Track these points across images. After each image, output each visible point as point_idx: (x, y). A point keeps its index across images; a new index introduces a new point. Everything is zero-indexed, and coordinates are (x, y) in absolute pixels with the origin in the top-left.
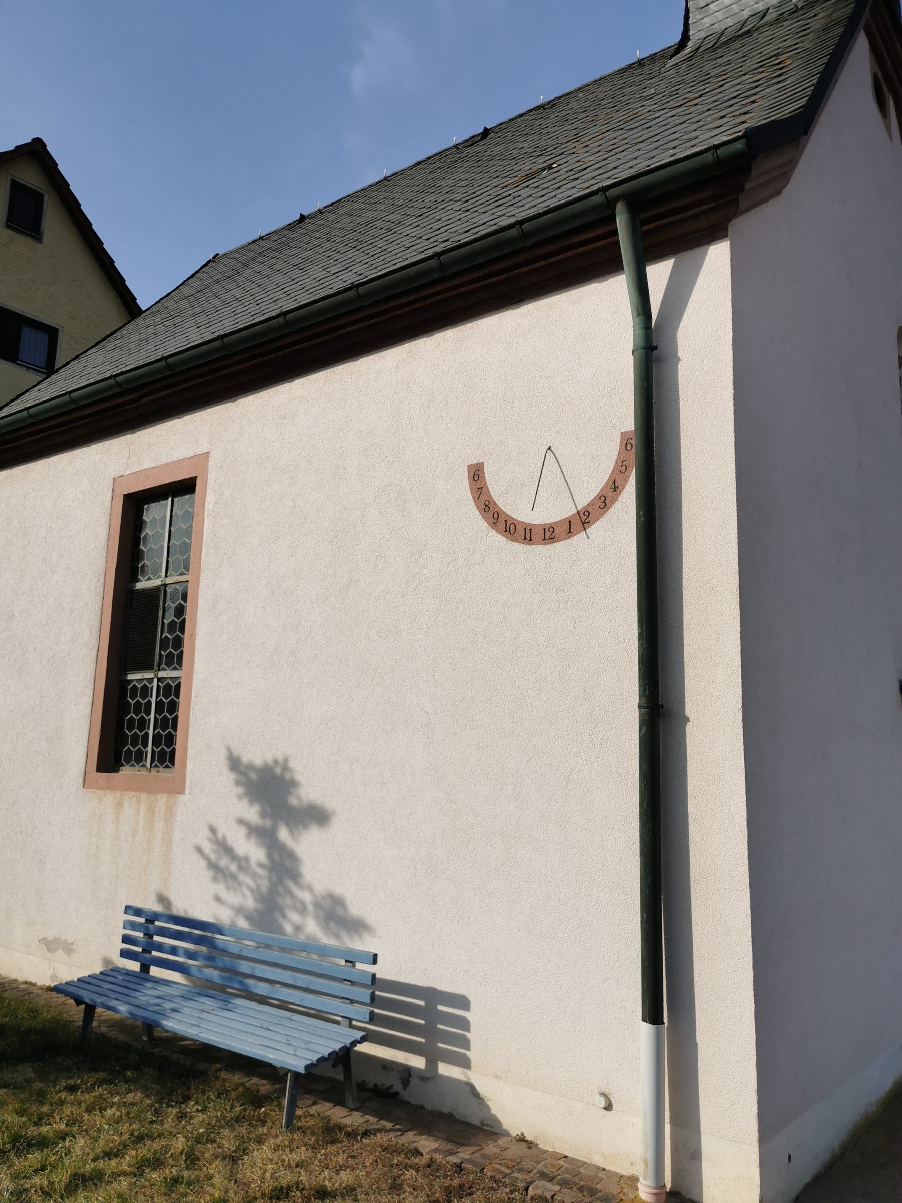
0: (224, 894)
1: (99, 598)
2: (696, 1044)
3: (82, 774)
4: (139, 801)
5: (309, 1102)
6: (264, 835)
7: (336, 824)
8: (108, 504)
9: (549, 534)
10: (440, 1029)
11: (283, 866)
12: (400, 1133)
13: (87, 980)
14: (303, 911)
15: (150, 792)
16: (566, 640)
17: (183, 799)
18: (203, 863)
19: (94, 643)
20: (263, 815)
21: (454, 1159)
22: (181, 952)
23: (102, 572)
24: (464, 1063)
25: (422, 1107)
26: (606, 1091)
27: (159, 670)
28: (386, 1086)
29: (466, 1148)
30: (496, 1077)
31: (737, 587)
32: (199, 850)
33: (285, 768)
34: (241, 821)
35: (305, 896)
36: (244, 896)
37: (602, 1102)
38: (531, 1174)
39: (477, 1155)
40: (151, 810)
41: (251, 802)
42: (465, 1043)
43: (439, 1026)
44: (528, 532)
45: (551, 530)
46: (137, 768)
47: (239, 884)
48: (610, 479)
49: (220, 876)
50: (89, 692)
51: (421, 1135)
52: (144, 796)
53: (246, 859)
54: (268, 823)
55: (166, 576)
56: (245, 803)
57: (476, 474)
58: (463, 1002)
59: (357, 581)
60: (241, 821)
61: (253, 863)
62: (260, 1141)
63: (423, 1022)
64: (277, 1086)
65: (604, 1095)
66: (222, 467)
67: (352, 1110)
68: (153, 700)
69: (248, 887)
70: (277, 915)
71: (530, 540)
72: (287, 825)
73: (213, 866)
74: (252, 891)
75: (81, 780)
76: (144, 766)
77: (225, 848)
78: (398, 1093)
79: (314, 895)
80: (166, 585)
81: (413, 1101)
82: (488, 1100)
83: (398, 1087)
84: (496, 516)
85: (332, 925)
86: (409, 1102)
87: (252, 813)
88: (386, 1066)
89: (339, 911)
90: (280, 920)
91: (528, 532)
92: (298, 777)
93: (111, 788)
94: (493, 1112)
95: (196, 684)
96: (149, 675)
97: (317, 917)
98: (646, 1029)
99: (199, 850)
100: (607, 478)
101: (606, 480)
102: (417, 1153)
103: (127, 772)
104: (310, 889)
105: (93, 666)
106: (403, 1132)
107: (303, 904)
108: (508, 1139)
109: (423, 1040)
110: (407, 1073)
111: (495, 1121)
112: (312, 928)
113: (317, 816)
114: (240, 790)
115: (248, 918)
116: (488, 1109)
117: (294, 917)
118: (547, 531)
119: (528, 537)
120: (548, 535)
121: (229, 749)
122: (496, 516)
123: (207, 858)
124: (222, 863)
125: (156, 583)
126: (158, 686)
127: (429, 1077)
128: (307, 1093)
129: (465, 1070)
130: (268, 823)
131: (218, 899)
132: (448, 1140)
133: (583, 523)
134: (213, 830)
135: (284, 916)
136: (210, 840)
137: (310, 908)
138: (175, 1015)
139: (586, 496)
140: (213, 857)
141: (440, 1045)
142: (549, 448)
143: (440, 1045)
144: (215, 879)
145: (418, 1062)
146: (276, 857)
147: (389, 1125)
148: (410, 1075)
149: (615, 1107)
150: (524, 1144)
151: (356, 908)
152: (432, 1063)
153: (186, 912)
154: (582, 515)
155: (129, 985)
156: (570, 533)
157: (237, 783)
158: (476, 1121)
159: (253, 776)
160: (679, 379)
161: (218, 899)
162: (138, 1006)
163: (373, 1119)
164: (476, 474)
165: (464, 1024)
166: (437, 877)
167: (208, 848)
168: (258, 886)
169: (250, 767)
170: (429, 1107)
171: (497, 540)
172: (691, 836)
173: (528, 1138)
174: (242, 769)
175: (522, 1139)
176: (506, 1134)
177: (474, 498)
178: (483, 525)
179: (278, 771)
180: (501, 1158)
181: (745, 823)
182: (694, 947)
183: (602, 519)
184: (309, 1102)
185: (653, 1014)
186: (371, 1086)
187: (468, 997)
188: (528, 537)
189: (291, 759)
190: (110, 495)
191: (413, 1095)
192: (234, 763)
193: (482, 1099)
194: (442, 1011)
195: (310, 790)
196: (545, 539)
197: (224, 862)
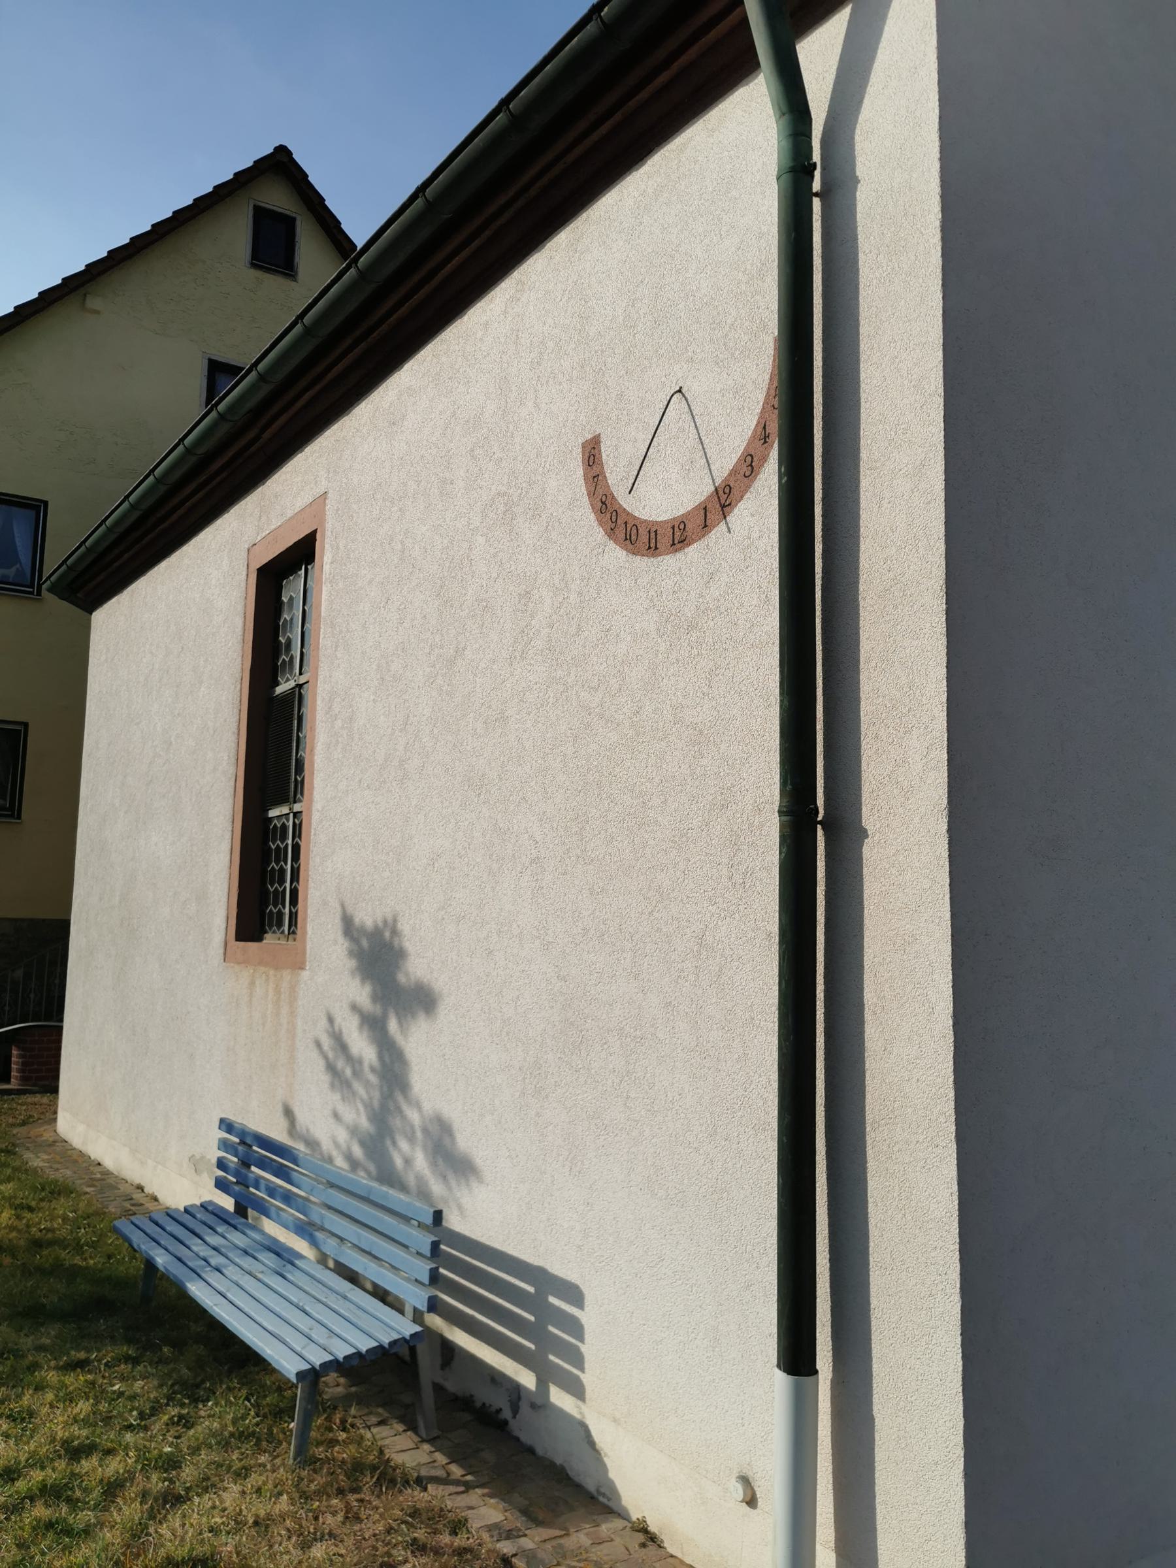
0: (342, 1109)
1: (236, 711)
2: (872, 1419)
3: (223, 944)
4: (267, 980)
5: (374, 1419)
6: (374, 1025)
7: (444, 1011)
8: (243, 584)
9: (678, 535)
10: (550, 1332)
11: (393, 1072)
12: (462, 1489)
13: (175, 1216)
14: (411, 1139)
15: (276, 968)
16: (699, 709)
17: (305, 974)
18: (321, 1063)
19: (232, 770)
20: (375, 998)
21: (506, 1547)
22: (263, 1187)
23: (238, 676)
24: (577, 1390)
25: (531, 1451)
26: (750, 1474)
27: (295, 802)
28: (493, 1409)
29: (540, 1530)
30: (615, 1420)
31: (942, 582)
32: (318, 1044)
33: (395, 932)
34: (354, 1008)
35: (414, 1116)
36: (358, 1113)
37: (738, 1491)
39: (548, 1546)
40: (277, 991)
41: (363, 981)
42: (578, 1360)
43: (551, 1329)
44: (653, 535)
45: (682, 526)
46: (278, 935)
47: (354, 1094)
48: (758, 423)
49: (337, 1083)
50: (228, 835)
51: (491, 1496)
52: (272, 972)
53: (360, 1061)
54: (378, 1010)
55: (301, 674)
56: (357, 981)
57: (592, 454)
58: (574, 1294)
59: (464, 649)
60: (354, 1008)
62: (242, 1474)
63: (532, 1318)
64: (353, 1389)
65: (745, 1481)
66: (337, 510)
67: (423, 1441)
68: (290, 842)
69: (362, 1100)
70: (388, 1143)
71: (656, 548)
72: (397, 1014)
73: (331, 1068)
74: (366, 1106)
75: (222, 951)
76: (283, 932)
77: (342, 1046)
78: (506, 1422)
79: (422, 1116)
80: (300, 686)
82: (606, 1455)
83: (507, 1414)
84: (614, 518)
85: (440, 1162)
86: (518, 1439)
87: (361, 993)
88: (496, 1378)
89: (447, 1141)
90: (391, 1149)
91: (653, 535)
92: (409, 945)
93: (245, 962)
94: (612, 1475)
95: (316, 817)
96: (285, 810)
98: (781, 1380)
99: (318, 1044)
100: (755, 422)
101: (752, 428)
102: (457, 1526)
103: (269, 939)
104: (418, 1106)
105: (231, 801)
106: (469, 1487)
107: (412, 1127)
108: (618, 1523)
109: (533, 1347)
110: (516, 1391)
111: (614, 1493)
112: (421, 1162)
113: (422, 1000)
114: (353, 963)
115: (362, 1144)
116: (604, 1468)
117: (404, 1145)
118: (676, 529)
119: (653, 545)
120: (677, 534)
121: (343, 906)
122: (614, 518)
123: (326, 1058)
124: (339, 1068)
125: (292, 684)
126: (294, 823)
127: (540, 1404)
128: (378, 1406)
129: (579, 1403)
130: (378, 1010)
131: (336, 1116)
132: (525, 1512)
133: (723, 507)
134: (331, 1020)
135: (394, 1143)
136: (328, 1032)
137: (419, 1134)
138: (213, 1278)
139: (725, 462)
140: (331, 1055)
141: (551, 1357)
142: (680, 391)
143: (551, 1357)
144: (332, 1086)
145: (527, 1379)
146: (387, 1060)
147: (456, 1471)
148: (519, 1398)
149: (760, 1502)
150: (641, 1537)
151: (465, 1141)
152: (542, 1383)
153: (308, 1130)
154: (721, 492)
155: (200, 1229)
156: (706, 527)
157: (351, 953)
158: (591, 1486)
159: (365, 943)
160: (859, 216)
161: (336, 1116)
162: (180, 1260)
163: (441, 1458)
164: (592, 454)
165: (577, 1329)
166: (547, 1096)
168: (371, 1098)
169: (362, 930)
170: (540, 1452)
171: (616, 554)
172: (868, 1044)
173: (653, 1528)
174: (355, 934)
175: (642, 1528)
176: (622, 1515)
177: (589, 494)
178: (599, 534)
179: (387, 934)
180: (584, 1556)
181: (951, 1022)
182: (871, 1244)
183: (748, 495)
184: (374, 1419)
185: (796, 1357)
186: (478, 1404)
187: (582, 1287)
188: (653, 545)
189: (400, 918)
190: (245, 573)
191: (524, 1427)
192: (349, 926)
195: (419, 966)
196: (674, 544)
197: (340, 1064)
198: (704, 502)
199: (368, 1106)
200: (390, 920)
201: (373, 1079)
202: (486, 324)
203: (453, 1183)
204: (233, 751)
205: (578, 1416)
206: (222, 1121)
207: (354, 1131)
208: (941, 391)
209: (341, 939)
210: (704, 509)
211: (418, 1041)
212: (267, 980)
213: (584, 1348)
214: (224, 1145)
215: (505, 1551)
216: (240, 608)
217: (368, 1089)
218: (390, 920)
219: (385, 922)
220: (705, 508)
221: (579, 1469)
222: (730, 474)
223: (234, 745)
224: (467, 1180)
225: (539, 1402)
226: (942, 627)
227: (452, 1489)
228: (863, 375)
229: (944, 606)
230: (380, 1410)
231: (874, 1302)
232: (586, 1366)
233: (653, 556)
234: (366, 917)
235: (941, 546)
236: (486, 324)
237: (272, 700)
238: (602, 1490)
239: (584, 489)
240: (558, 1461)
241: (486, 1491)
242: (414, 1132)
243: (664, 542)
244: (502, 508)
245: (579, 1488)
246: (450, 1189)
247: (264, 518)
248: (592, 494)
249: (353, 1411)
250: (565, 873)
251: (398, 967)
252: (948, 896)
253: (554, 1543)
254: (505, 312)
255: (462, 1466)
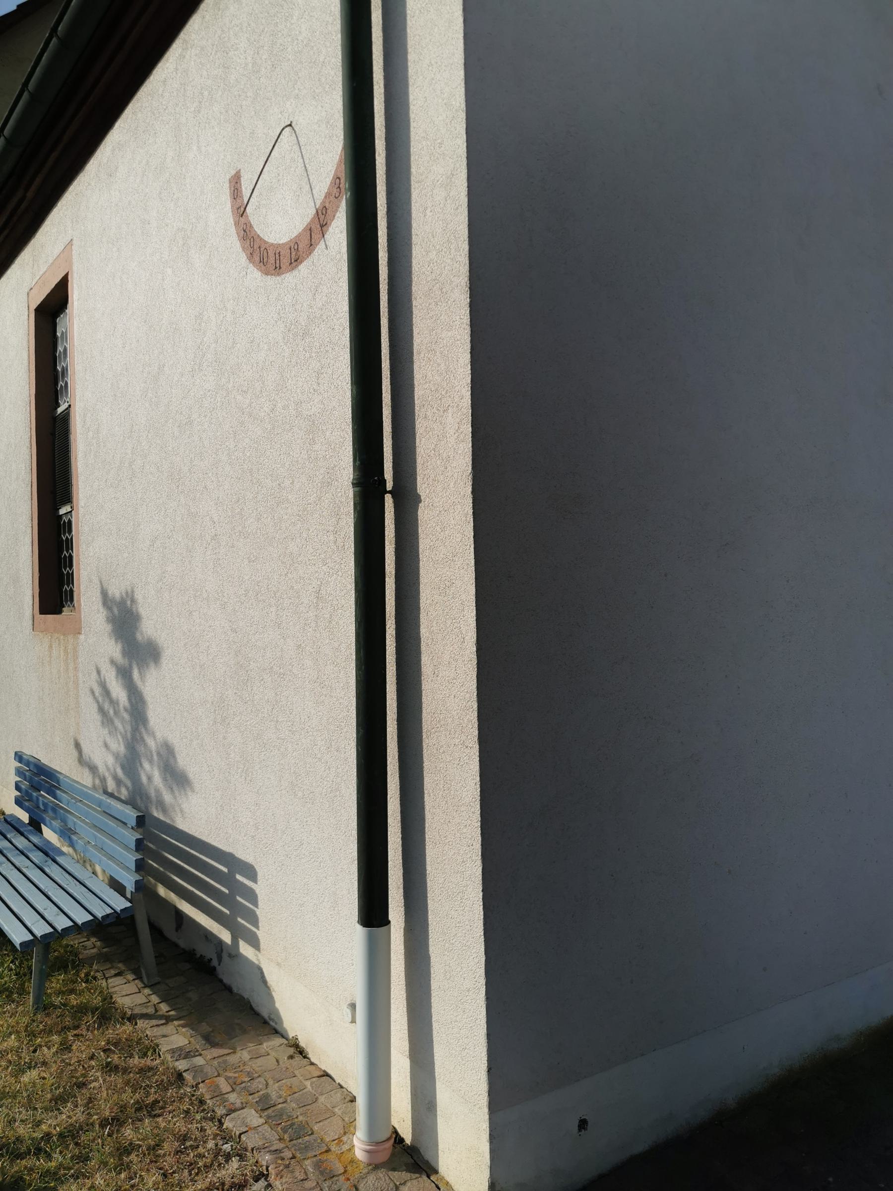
1: (28, 429)
6: (124, 674)
7: (165, 660)
8: (26, 323)
12: (163, 1021)
14: (151, 762)
18: (95, 706)
20: (125, 653)
21: (181, 1065)
23: (27, 400)
24: (255, 943)
25: (229, 989)
28: (206, 959)
29: (213, 1050)
30: (278, 964)
32: (93, 692)
33: (133, 601)
35: (151, 743)
36: (119, 744)
38: (251, 1097)
42: (255, 921)
47: (116, 729)
51: (183, 1026)
56: (113, 642)
58: (250, 872)
59: (164, 365)
60: (113, 662)
61: (121, 706)
69: (121, 733)
73: (101, 710)
74: (123, 738)
75: (31, 622)
77: (107, 692)
79: (156, 743)
81: (225, 981)
83: (215, 963)
85: (168, 776)
86: (221, 981)
87: (113, 649)
88: (208, 936)
89: (172, 761)
90: (139, 769)
94: (277, 1005)
97: (159, 767)
98: (359, 932)
99: (93, 692)
104: (153, 735)
106: (168, 1019)
109: (228, 912)
114: (109, 627)
123: (98, 702)
127: (235, 955)
129: (257, 952)
131: (106, 745)
133: (322, 226)
134: (99, 672)
136: (97, 682)
137: (155, 757)
140: (100, 699)
142: (290, 125)
145: (226, 936)
146: (133, 701)
147: (164, 1008)
148: (222, 950)
150: (292, 1051)
151: (183, 761)
152: (235, 938)
156: (311, 246)
158: (265, 1014)
159: (116, 611)
161: (106, 745)
163: (155, 999)
167: (98, 690)
169: (113, 600)
170: (235, 990)
171: (255, 274)
172: (424, 669)
173: (302, 1044)
178: (243, 258)
179: (129, 602)
185: (373, 912)
190: (26, 313)
193: (268, 988)
194: (239, 881)
195: (150, 627)
196: (291, 263)
197: (106, 706)
198: (309, 224)
199: (124, 737)
200: (129, 591)
201: (126, 716)
202: (165, 81)
203: (177, 793)
204: (28, 462)
205: (256, 962)
206: (16, 753)
207: (117, 756)
208: (463, 106)
209: (101, 609)
210: (310, 230)
211: (152, 684)
212: (59, 644)
213: (258, 912)
214: (19, 772)
215: (180, 1067)
216: (25, 344)
217: (123, 725)
218: (129, 591)
219: (127, 593)
220: (310, 230)
221: (257, 1001)
222: (326, 197)
223: (28, 457)
224: (185, 790)
225: (233, 953)
226: (466, 319)
227: (154, 1022)
228: (411, 97)
229: (468, 300)
230: (120, 965)
231: (429, 868)
232: (260, 925)
233: (279, 274)
234: (115, 591)
235: (466, 247)
236: (165, 81)
237: (55, 419)
238: (272, 1016)
239: (232, 220)
240: (246, 997)
241: (181, 1022)
242: (152, 756)
243: (285, 261)
244: (181, 242)
245: (257, 1014)
246: (175, 798)
247: (35, 266)
248: (237, 224)
249: (95, 967)
250: (233, 546)
251: (137, 628)
252: (473, 546)
253: (220, 1060)
254: (177, 69)
255: (169, 1005)
